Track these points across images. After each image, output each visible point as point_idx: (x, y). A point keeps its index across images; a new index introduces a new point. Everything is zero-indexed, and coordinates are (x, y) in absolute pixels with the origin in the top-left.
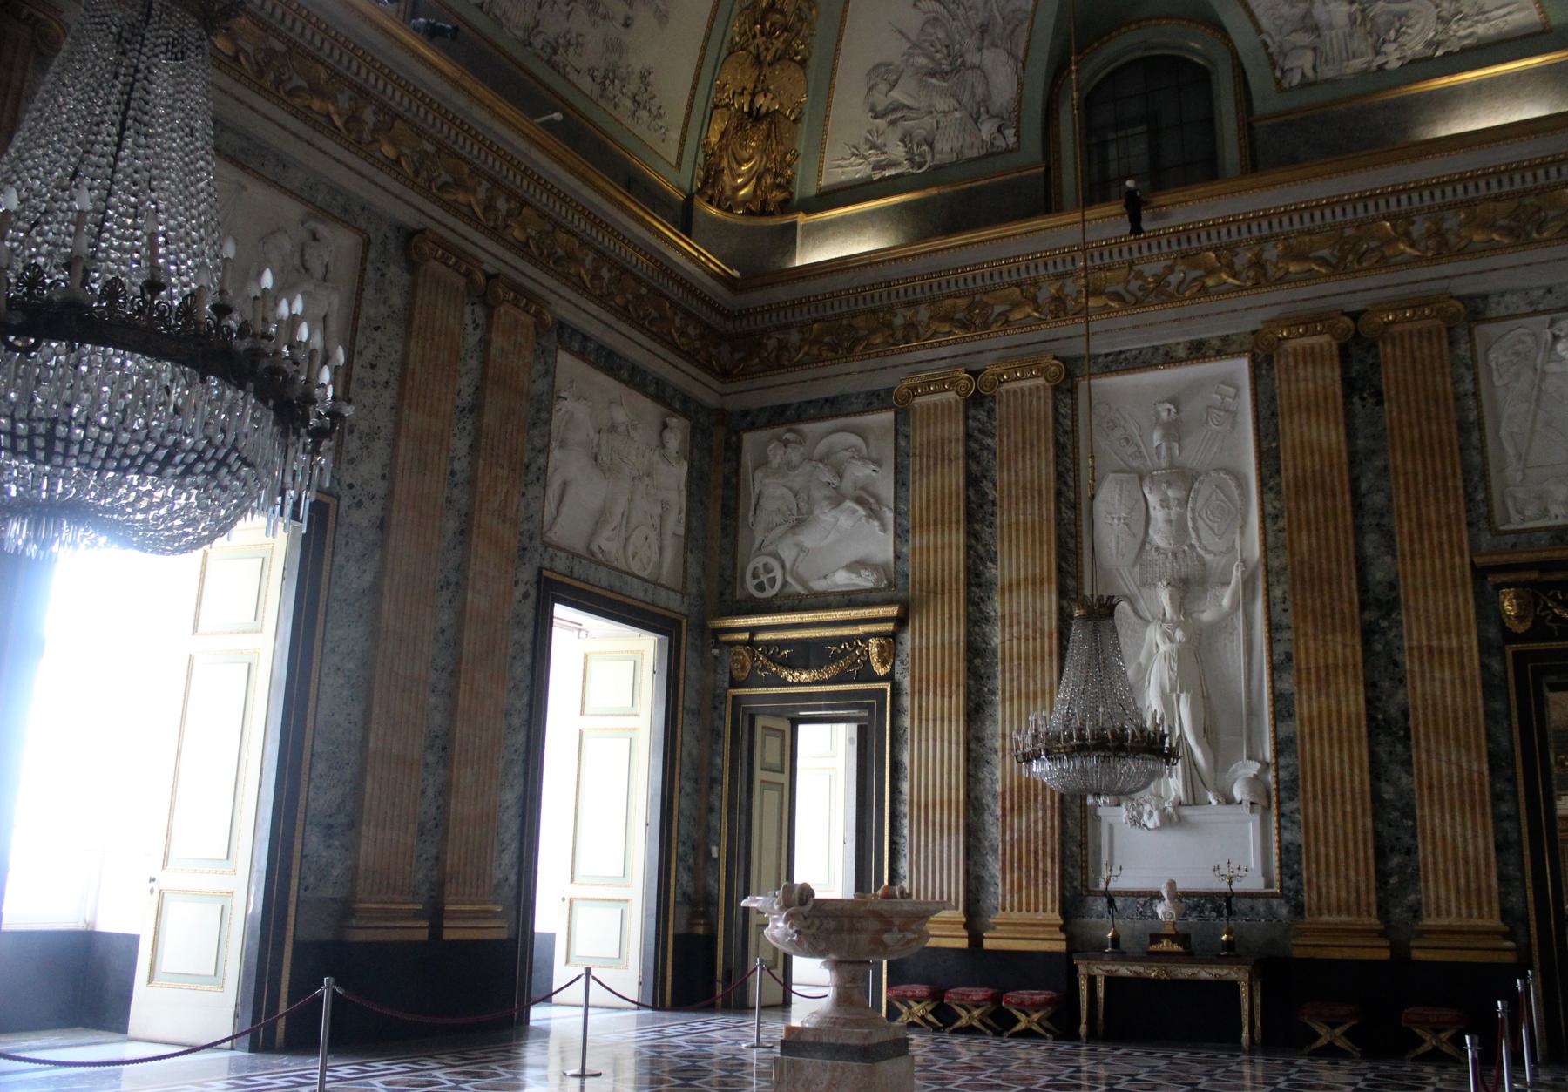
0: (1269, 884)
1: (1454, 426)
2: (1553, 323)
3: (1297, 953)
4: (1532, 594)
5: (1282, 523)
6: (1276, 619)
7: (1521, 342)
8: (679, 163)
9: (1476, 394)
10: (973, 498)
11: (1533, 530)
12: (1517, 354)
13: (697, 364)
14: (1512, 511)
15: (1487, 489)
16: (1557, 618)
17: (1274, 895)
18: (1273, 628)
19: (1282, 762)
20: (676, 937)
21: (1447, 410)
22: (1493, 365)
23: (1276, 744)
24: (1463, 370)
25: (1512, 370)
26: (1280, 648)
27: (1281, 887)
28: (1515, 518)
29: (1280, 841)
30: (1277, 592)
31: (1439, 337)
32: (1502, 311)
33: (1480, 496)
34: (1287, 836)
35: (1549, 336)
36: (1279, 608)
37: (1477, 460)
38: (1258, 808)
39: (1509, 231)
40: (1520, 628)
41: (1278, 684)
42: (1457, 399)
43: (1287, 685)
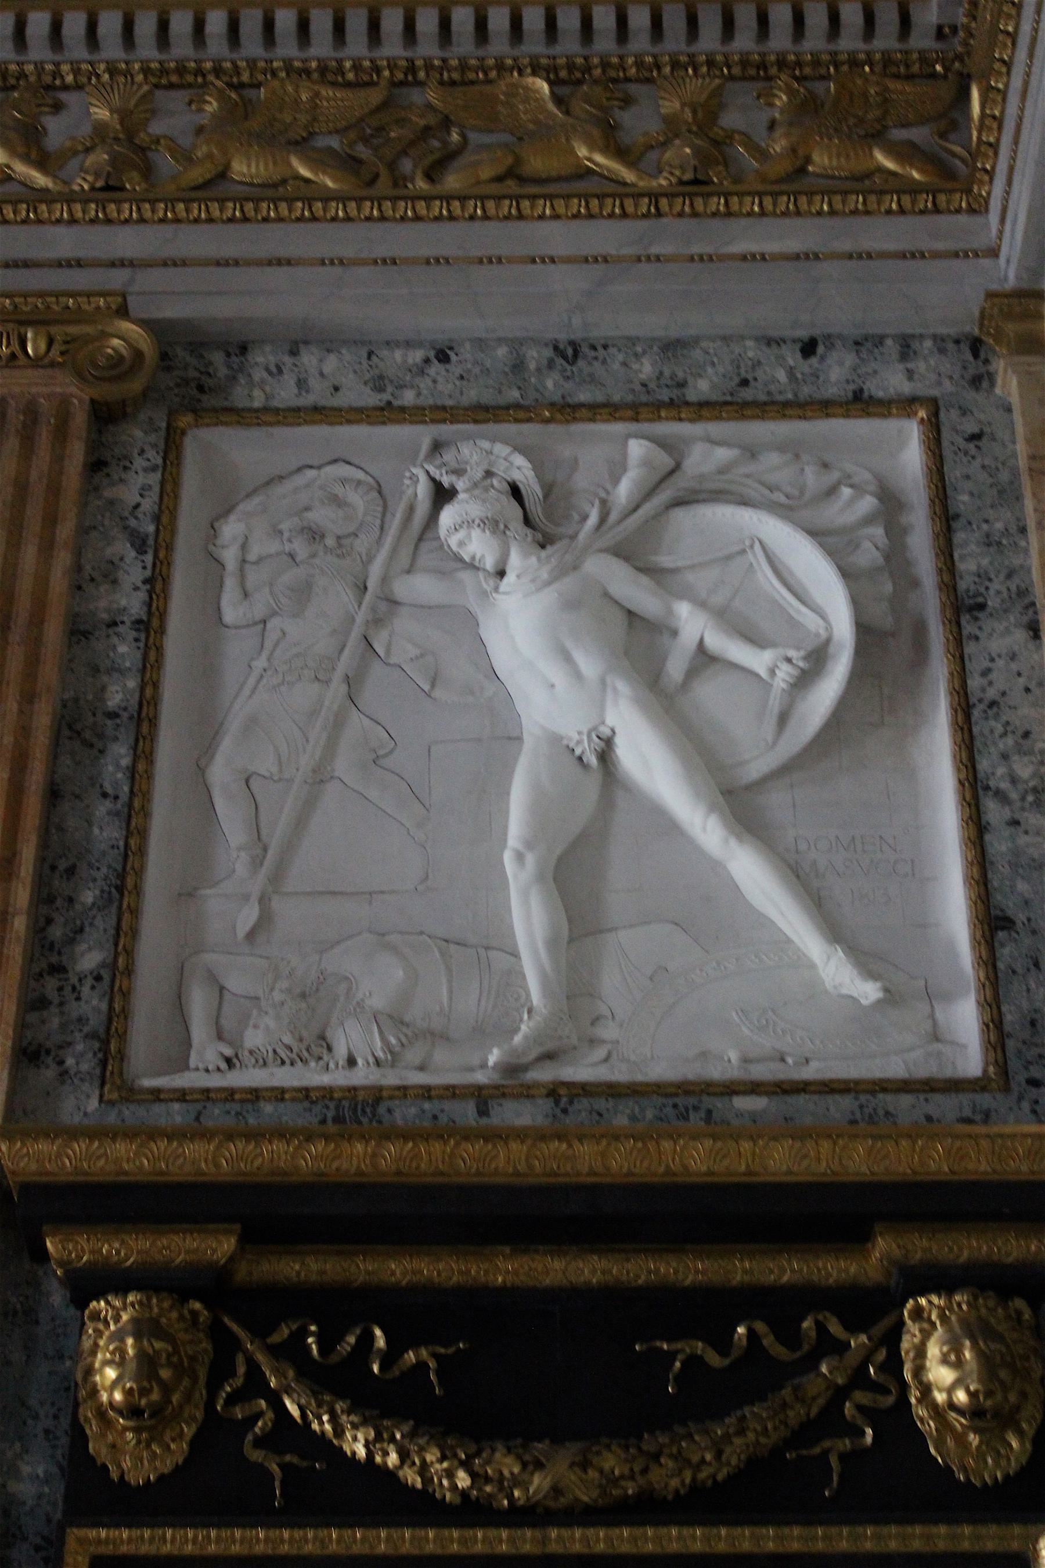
1: (43, 719)
2: (437, 447)
4: (216, 1322)
7: (338, 502)
9: (151, 627)
11: (255, 1095)
12: (314, 535)
14: (199, 1031)
15: (124, 938)
16: (288, 1434)
21: (33, 662)
22: (230, 556)
24: (123, 548)
25: (290, 576)
28: (206, 1051)
31: (61, 434)
32: (286, 394)
33: (89, 958)
35: (423, 490)
37: (106, 833)
39: (349, 164)
40: (134, 1460)
42: (79, 632)
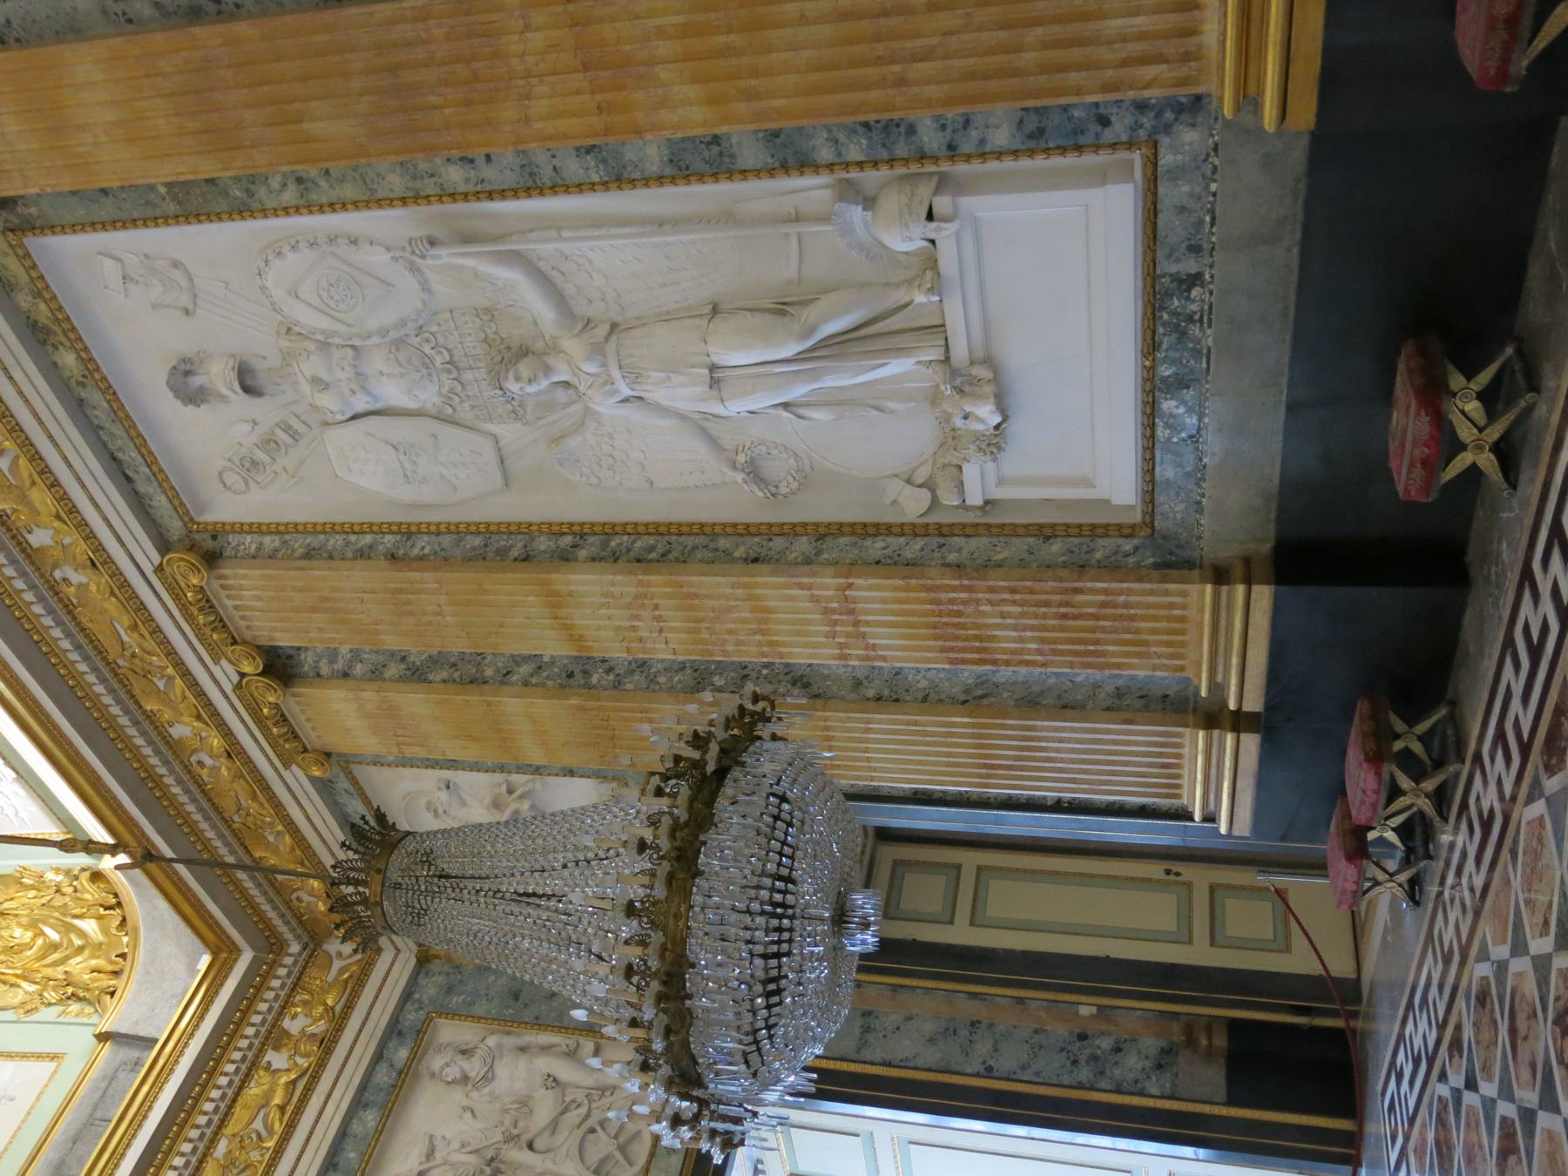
0: (1125, 174)
3: (1305, 114)
5: (312, 172)
6: (511, 179)
8: (53, 1057)
10: (444, 675)
13: (349, 1006)
17: (1152, 163)
18: (531, 187)
19: (826, 154)
20: (1232, 1101)
23: (785, 168)
26: (573, 168)
27: (1130, 145)
29: (1015, 153)
30: (455, 176)
34: (1002, 137)
36: (488, 173)
38: (942, 204)
41: (653, 168)
43: (652, 154)
